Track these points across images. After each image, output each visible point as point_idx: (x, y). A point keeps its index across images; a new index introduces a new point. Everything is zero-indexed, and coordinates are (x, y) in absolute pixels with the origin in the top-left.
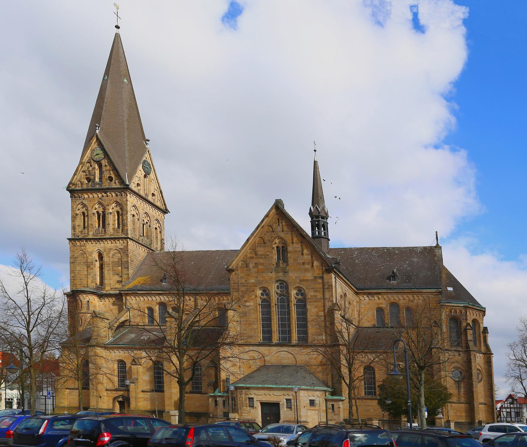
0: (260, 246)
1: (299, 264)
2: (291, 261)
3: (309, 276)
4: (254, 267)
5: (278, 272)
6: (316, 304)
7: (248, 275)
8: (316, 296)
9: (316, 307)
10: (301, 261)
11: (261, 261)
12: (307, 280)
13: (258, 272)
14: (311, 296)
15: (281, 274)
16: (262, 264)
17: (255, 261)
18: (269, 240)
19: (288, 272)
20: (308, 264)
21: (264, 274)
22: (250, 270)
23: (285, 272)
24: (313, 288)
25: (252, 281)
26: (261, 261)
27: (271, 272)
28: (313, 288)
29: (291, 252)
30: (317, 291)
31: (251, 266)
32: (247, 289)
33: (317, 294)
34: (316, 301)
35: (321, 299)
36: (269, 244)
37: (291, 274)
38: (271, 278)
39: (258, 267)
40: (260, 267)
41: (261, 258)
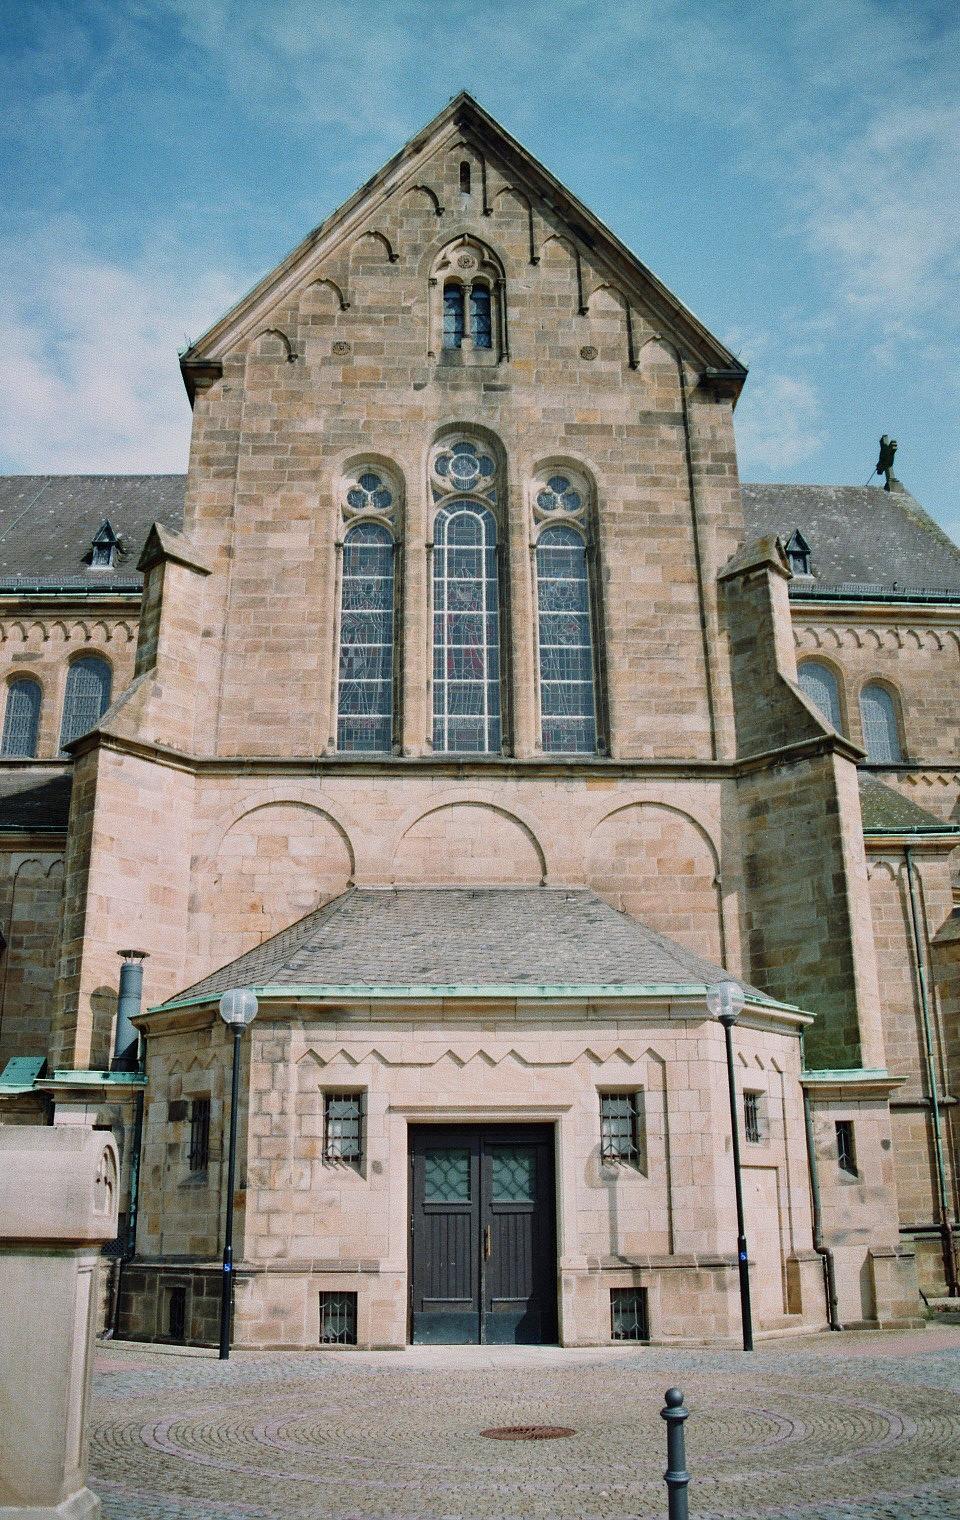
0: (371, 272)
1: (565, 353)
2: (518, 340)
3: (618, 407)
4: (325, 361)
5: (456, 388)
6: (652, 544)
7: (294, 396)
8: (651, 506)
9: (652, 559)
10: (576, 343)
11: (369, 333)
12: (605, 429)
13: (347, 384)
14: (627, 505)
20: (610, 354)
21: (379, 395)
22: (305, 374)
24: (635, 468)
25: (314, 425)
26: (369, 333)
27: (418, 387)
28: (635, 468)
29: (521, 300)
30: (656, 482)
31: (312, 354)
32: (280, 464)
33: (656, 495)
34: (651, 533)
35: (678, 519)
36: (409, 262)
37: (519, 398)
38: (416, 413)
40: (361, 361)
41: (370, 321)
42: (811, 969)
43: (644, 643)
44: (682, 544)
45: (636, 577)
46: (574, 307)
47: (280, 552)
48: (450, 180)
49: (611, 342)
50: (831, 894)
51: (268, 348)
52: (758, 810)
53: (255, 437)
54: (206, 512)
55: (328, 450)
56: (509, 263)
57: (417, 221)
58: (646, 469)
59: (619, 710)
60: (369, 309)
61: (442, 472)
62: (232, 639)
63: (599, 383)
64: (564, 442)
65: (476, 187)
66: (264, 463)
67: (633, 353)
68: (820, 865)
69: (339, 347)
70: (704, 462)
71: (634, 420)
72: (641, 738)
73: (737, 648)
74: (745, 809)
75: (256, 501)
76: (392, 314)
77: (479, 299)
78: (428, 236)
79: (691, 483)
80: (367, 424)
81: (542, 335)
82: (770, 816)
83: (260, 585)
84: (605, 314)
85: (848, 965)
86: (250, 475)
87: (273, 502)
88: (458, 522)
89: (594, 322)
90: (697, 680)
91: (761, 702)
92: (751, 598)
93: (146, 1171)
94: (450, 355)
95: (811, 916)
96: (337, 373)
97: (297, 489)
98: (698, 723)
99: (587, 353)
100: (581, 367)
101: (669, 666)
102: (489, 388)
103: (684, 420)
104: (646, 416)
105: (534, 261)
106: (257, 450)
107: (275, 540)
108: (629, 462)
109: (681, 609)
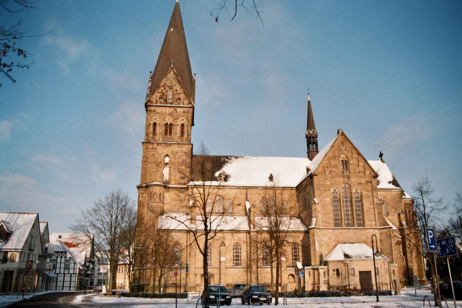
0: (332, 159)
1: (356, 172)
2: (351, 170)
3: (363, 181)
4: (329, 174)
5: (344, 178)
6: (368, 200)
7: (326, 179)
8: (368, 194)
9: (368, 202)
10: (358, 171)
11: (333, 169)
12: (362, 184)
15: (346, 179)
16: (334, 172)
17: (329, 169)
18: (338, 156)
19: (350, 178)
20: (362, 173)
22: (326, 176)
23: (349, 177)
24: (365, 189)
26: (333, 169)
27: (340, 178)
28: (365, 189)
29: (351, 164)
30: (368, 191)
31: (327, 172)
32: (325, 189)
33: (368, 193)
34: (368, 198)
35: (371, 196)
36: (337, 158)
38: (340, 182)
39: (331, 174)
40: (333, 173)
41: (333, 167)
42: (388, 252)
43: (368, 213)
44: (371, 200)
45: (367, 205)
46: (357, 165)
47: (326, 201)
48: (341, 144)
49: (362, 171)
50: (390, 244)
51: (322, 171)
52: (381, 234)
53: (322, 185)
54: (318, 195)
55: (330, 187)
56: (349, 158)
57: (337, 151)
58: (367, 189)
59: (366, 221)
60: (333, 165)
61: (343, 189)
62: (322, 213)
63: (361, 177)
64: (358, 186)
65: (344, 146)
66: (322, 189)
67: (365, 172)
68: (388, 241)
69: (330, 171)
70: (374, 188)
71: (365, 182)
72: (368, 225)
73: (378, 213)
74: (379, 233)
75: (323, 194)
76: (335, 166)
77: (345, 164)
78: (339, 154)
79: (372, 191)
80: (335, 183)
81: (354, 170)
82: (383, 235)
83: (325, 205)
84: (361, 166)
85: (392, 252)
86: (322, 190)
87: (325, 194)
88: (345, 196)
89: (360, 168)
90: (373, 217)
91: (381, 221)
92: (380, 208)
93: (330, 276)
94: (343, 172)
95: (388, 247)
96: (330, 175)
97: (327, 192)
98: (374, 223)
99: (359, 172)
100: (358, 175)
101: (371, 216)
102: (348, 178)
103: (371, 182)
104: (367, 182)
105: (352, 158)
106: (322, 187)
107: (326, 199)
108: (365, 188)
109: (372, 208)
